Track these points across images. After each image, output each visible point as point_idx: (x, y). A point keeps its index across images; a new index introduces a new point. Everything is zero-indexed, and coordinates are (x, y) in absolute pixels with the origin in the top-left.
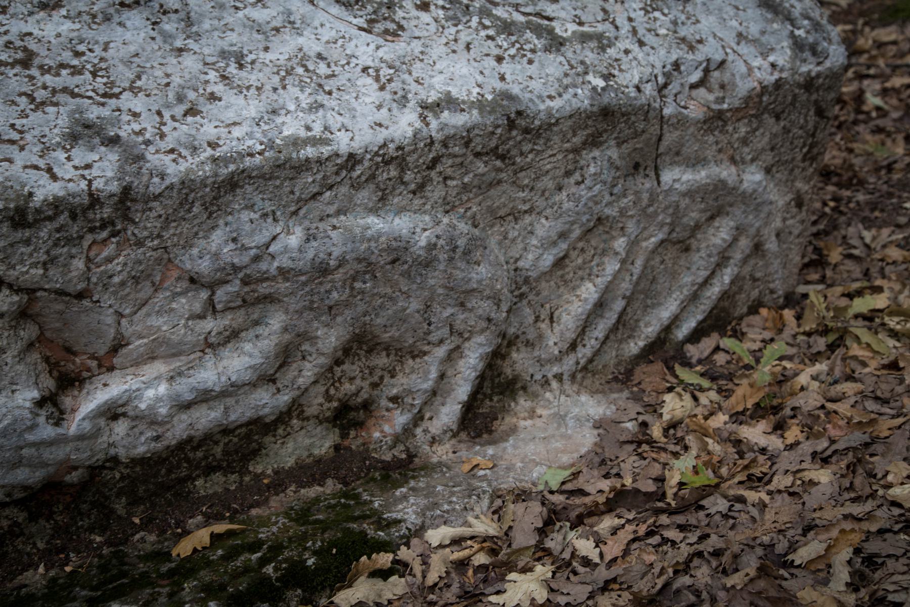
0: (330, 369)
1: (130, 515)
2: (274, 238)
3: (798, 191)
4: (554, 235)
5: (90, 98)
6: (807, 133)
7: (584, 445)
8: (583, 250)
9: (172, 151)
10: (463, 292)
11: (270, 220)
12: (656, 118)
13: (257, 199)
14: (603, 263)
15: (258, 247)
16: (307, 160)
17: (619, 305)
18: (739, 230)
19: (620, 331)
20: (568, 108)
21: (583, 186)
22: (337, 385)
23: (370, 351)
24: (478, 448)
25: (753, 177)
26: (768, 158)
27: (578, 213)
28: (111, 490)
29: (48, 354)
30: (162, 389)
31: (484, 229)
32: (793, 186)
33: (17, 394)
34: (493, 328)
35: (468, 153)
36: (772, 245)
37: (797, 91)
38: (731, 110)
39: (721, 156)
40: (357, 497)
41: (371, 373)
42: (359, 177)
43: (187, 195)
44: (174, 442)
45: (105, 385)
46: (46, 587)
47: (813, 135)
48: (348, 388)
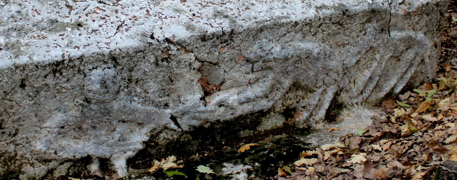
0: (284, 95)
1: (221, 141)
2: (272, 48)
3: (435, 42)
4: (356, 52)
5: (218, 4)
6: (438, 21)
7: (368, 124)
8: (365, 58)
9: (244, 20)
10: (328, 70)
11: (271, 42)
12: (389, 13)
13: (268, 35)
14: (372, 63)
15: (268, 50)
16: (283, 23)
17: (377, 78)
18: (417, 54)
19: (377, 89)
20: (361, 9)
21: (366, 36)
22: (286, 101)
23: (297, 90)
24: (332, 125)
25: (420, 36)
26: (425, 29)
27: (364, 45)
28: (216, 132)
29: (203, 84)
30: (236, 97)
31: (334, 49)
32: (433, 40)
33: (195, 95)
34: (337, 83)
35: (331, 23)
36: (427, 60)
37: (434, 6)
38: (412, 12)
39: (409, 28)
40: (294, 138)
41: (296, 98)
42: (298, 29)
43: (249, 33)
44: (237, 116)
45: (218, 95)
46: (200, 159)
47: (439, 22)
48: (289, 102)
